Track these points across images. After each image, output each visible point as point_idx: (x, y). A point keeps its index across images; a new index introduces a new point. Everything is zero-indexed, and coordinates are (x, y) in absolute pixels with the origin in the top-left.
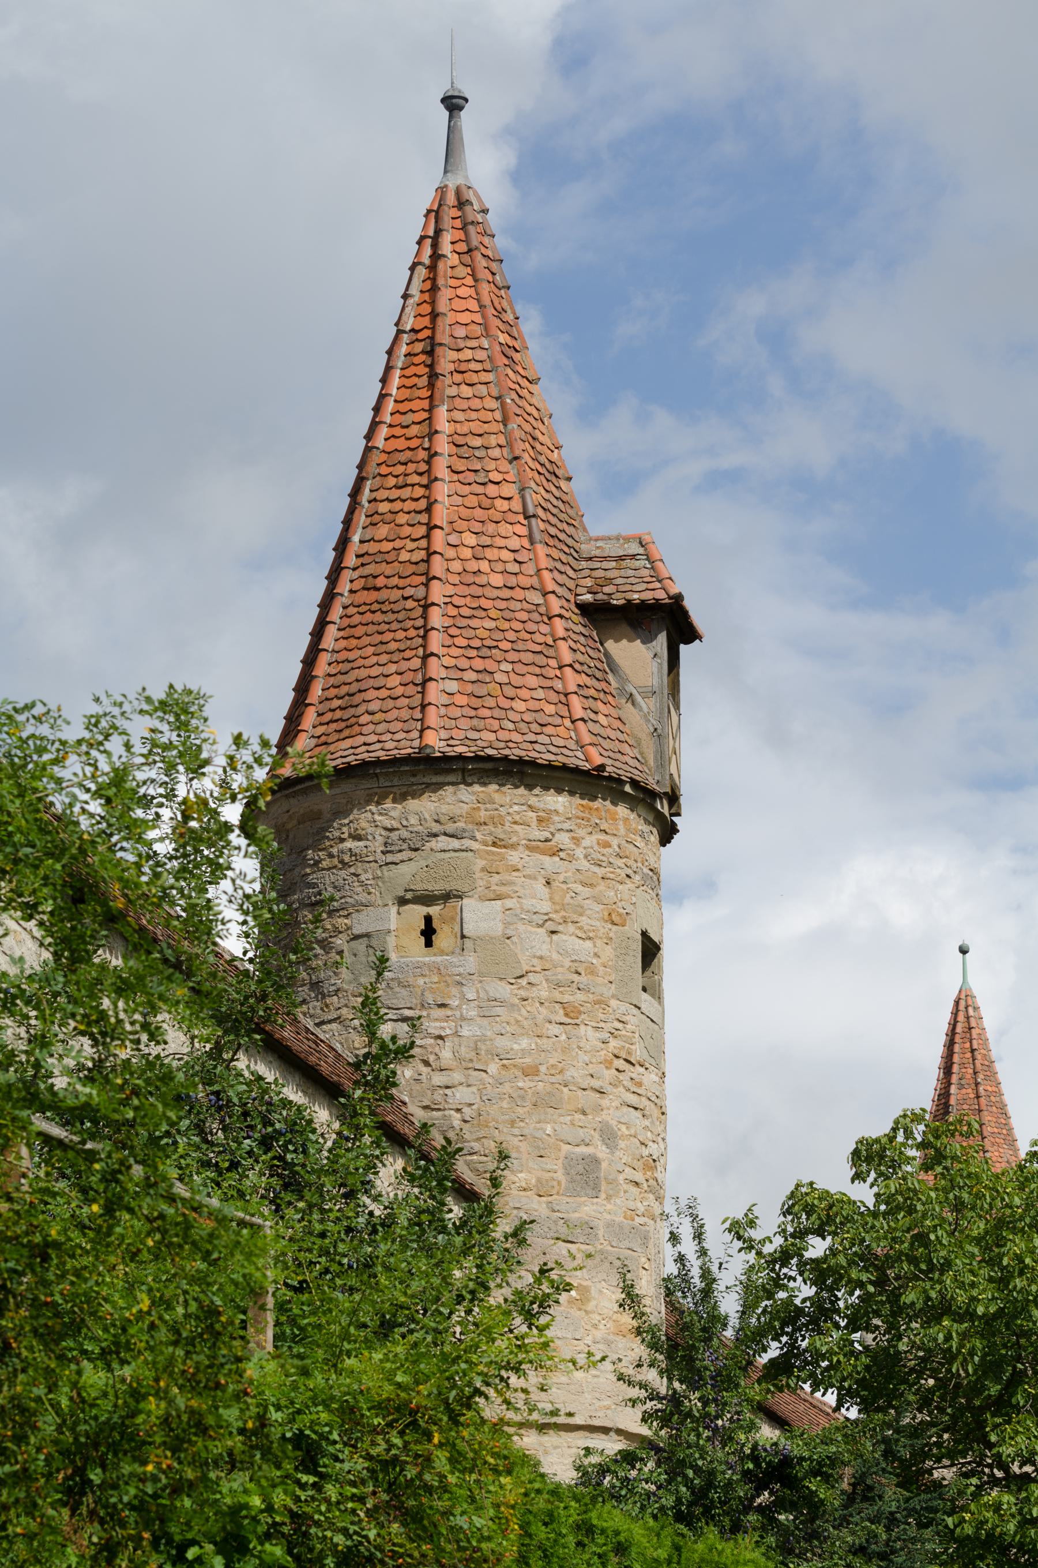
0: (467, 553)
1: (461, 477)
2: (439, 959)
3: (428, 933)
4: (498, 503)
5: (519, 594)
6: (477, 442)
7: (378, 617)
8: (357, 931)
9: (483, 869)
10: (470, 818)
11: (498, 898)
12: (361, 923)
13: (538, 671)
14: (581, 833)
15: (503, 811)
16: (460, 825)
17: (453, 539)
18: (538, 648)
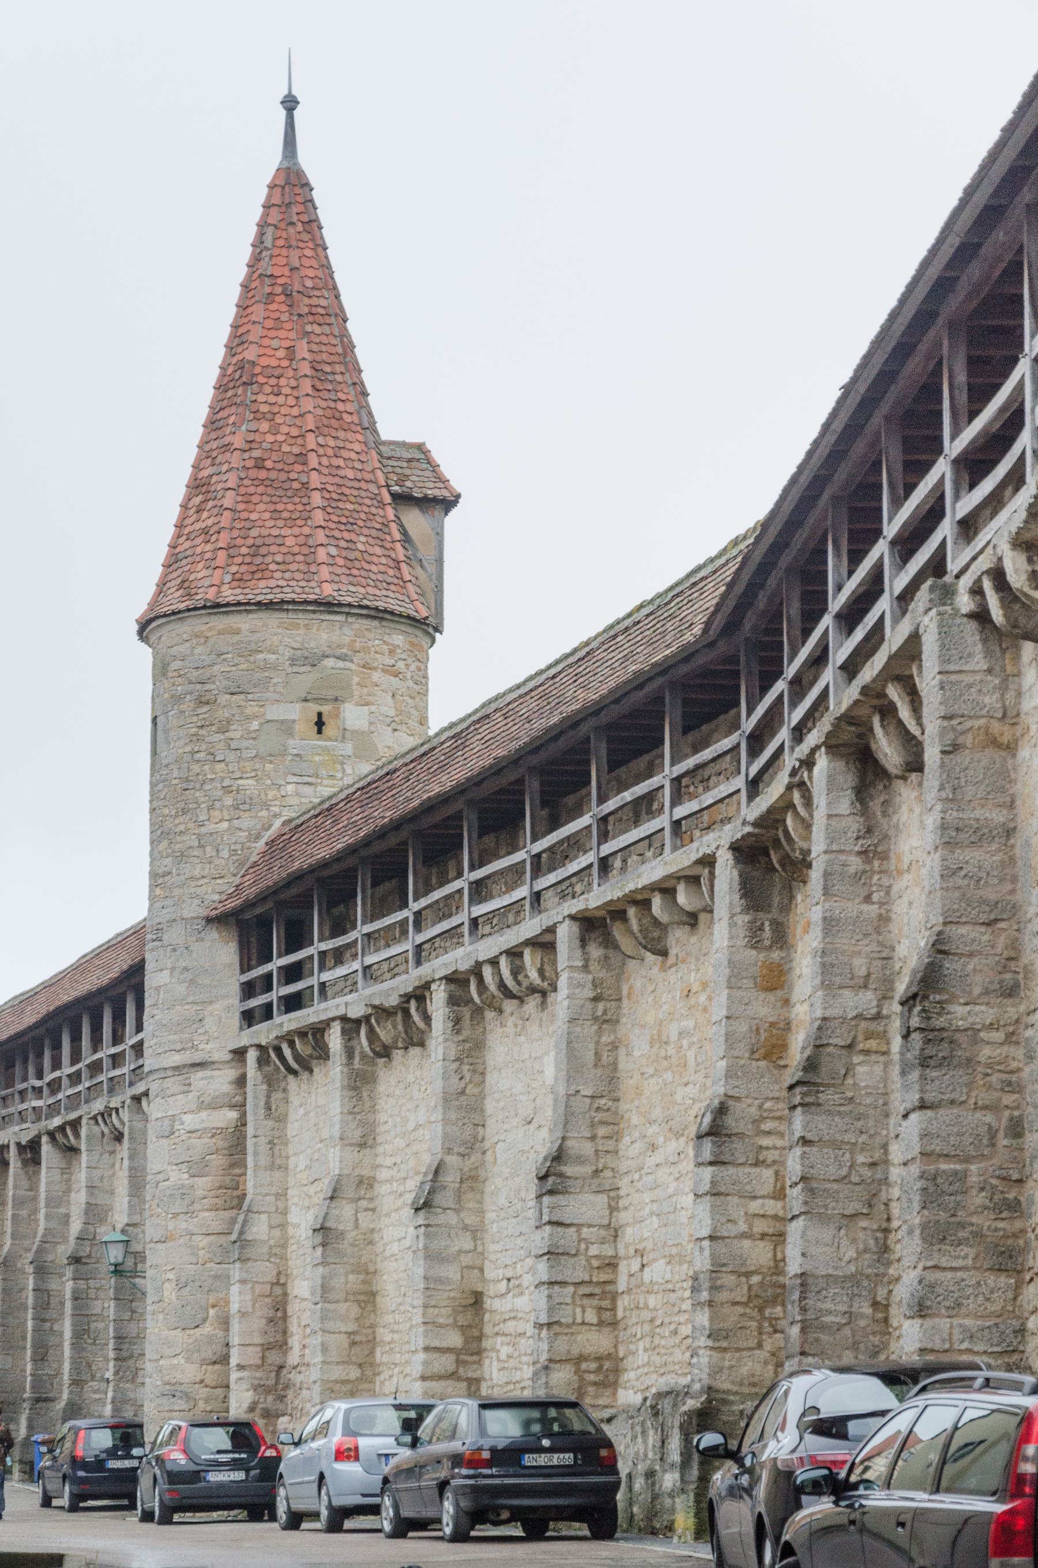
0: (330, 452)
1: (321, 394)
2: (329, 743)
3: (320, 724)
4: (345, 416)
5: (363, 485)
6: (328, 369)
7: (270, 490)
8: (268, 717)
9: (358, 684)
11: (367, 704)
13: (380, 543)
14: (410, 661)
15: (370, 643)
16: (344, 651)
17: (321, 440)
18: (379, 526)
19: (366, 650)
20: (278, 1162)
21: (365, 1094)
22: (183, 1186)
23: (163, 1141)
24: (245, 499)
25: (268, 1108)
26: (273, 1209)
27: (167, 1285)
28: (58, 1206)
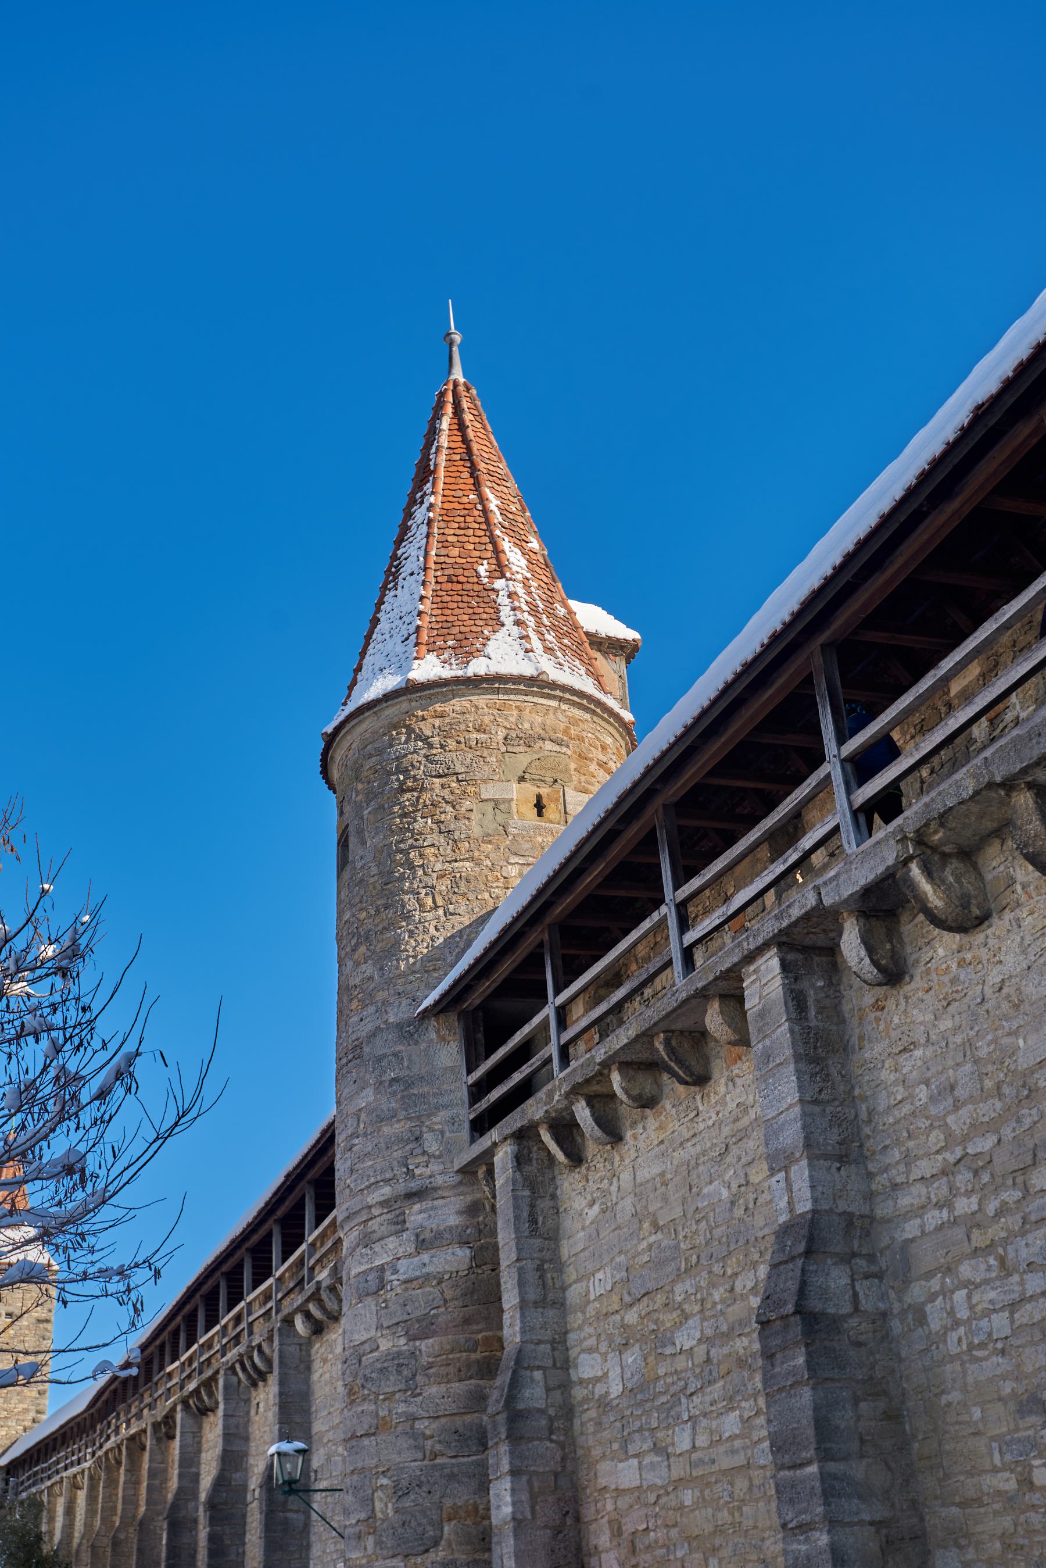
10: (566, 731)
12: (489, 791)
19: (581, 739)
20: (551, 1296)
21: (833, 1071)
22: (399, 1354)
23: (370, 1301)
24: (440, 605)
25: (533, 1221)
26: (550, 1363)
27: (379, 1494)
28: (190, 1466)
